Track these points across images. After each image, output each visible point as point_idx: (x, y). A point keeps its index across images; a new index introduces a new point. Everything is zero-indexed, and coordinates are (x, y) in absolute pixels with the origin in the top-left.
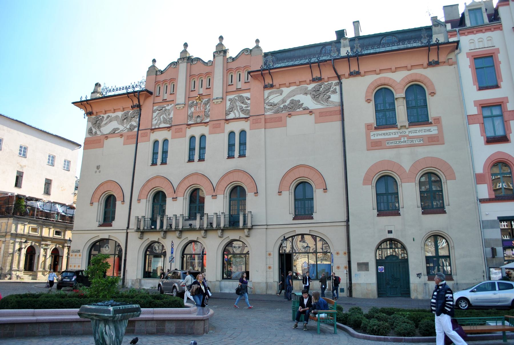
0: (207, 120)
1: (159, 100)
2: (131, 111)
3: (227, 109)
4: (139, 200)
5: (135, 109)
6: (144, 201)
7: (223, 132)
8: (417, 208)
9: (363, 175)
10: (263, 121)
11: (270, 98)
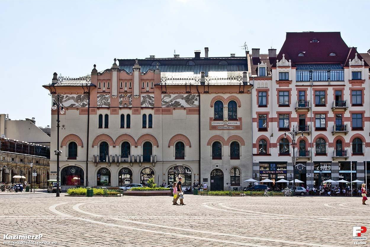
0: (131, 106)
1: (101, 91)
2: (83, 95)
3: (142, 101)
4: (93, 146)
5: (85, 94)
6: (96, 147)
7: (140, 114)
8: (229, 157)
9: (208, 141)
10: (161, 110)
11: (164, 98)
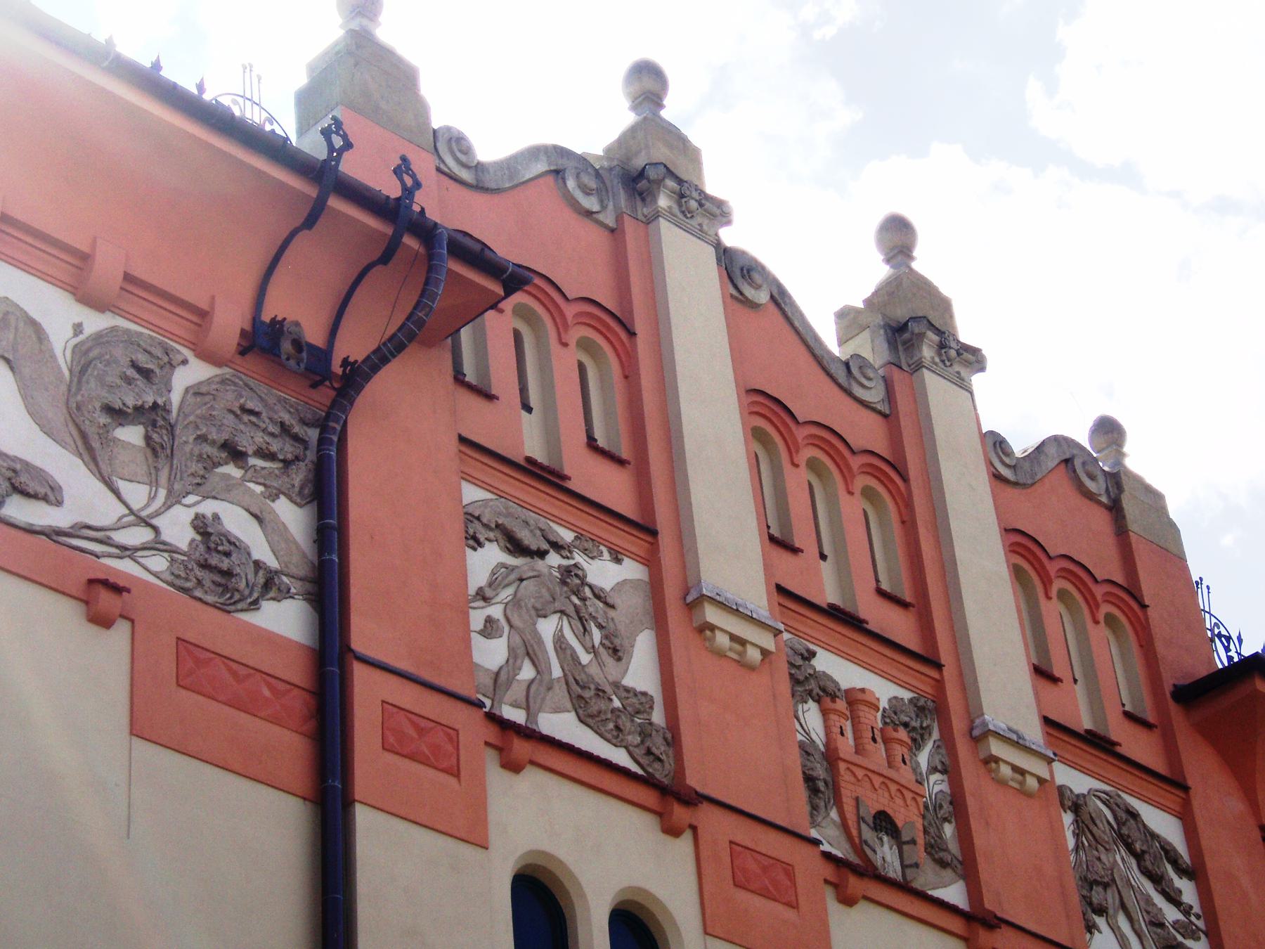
2: (192, 373)
